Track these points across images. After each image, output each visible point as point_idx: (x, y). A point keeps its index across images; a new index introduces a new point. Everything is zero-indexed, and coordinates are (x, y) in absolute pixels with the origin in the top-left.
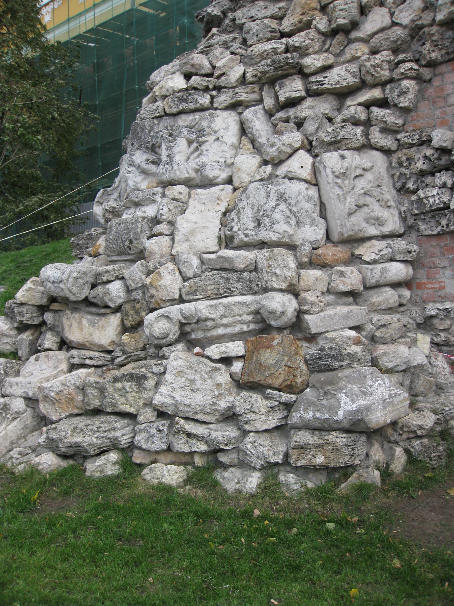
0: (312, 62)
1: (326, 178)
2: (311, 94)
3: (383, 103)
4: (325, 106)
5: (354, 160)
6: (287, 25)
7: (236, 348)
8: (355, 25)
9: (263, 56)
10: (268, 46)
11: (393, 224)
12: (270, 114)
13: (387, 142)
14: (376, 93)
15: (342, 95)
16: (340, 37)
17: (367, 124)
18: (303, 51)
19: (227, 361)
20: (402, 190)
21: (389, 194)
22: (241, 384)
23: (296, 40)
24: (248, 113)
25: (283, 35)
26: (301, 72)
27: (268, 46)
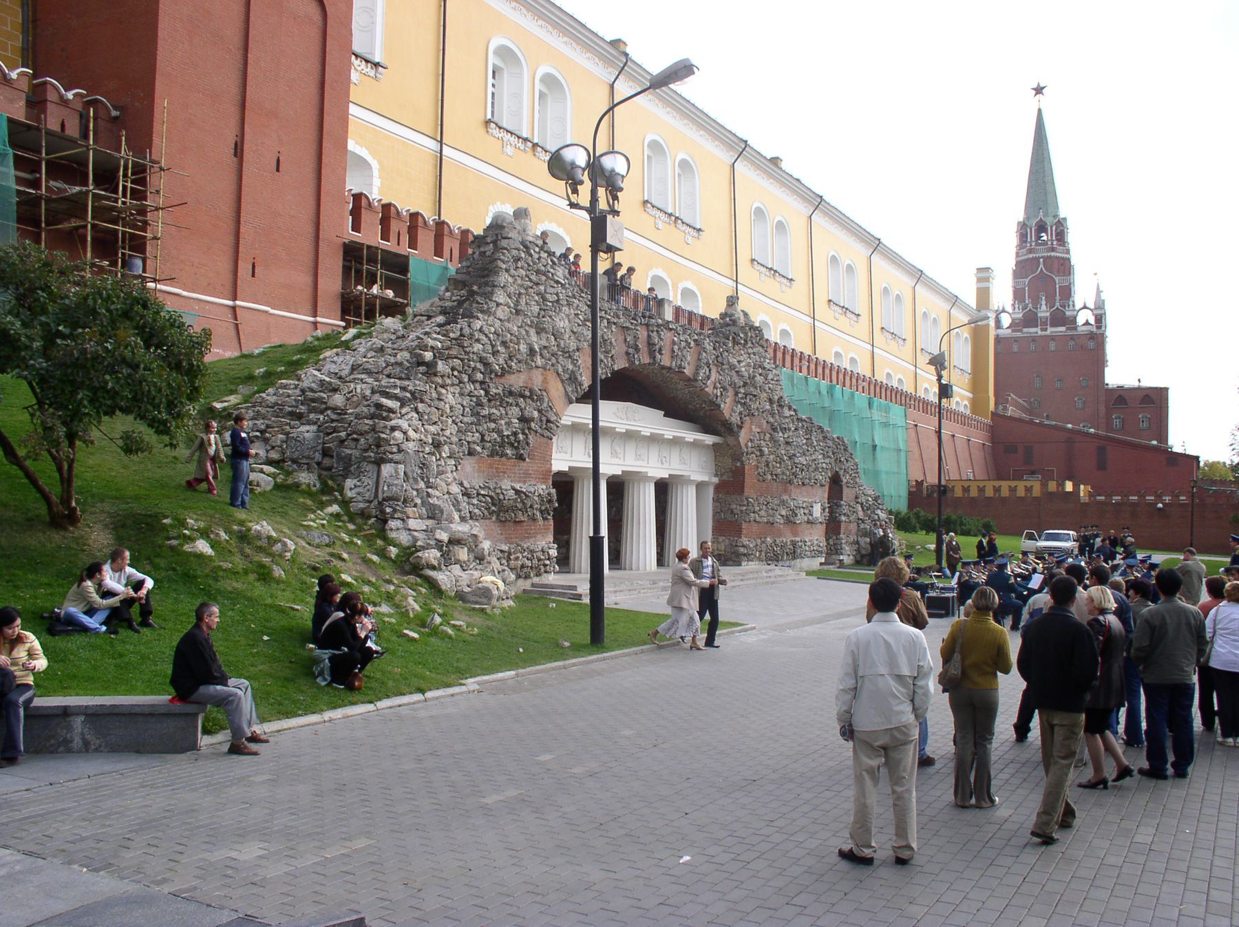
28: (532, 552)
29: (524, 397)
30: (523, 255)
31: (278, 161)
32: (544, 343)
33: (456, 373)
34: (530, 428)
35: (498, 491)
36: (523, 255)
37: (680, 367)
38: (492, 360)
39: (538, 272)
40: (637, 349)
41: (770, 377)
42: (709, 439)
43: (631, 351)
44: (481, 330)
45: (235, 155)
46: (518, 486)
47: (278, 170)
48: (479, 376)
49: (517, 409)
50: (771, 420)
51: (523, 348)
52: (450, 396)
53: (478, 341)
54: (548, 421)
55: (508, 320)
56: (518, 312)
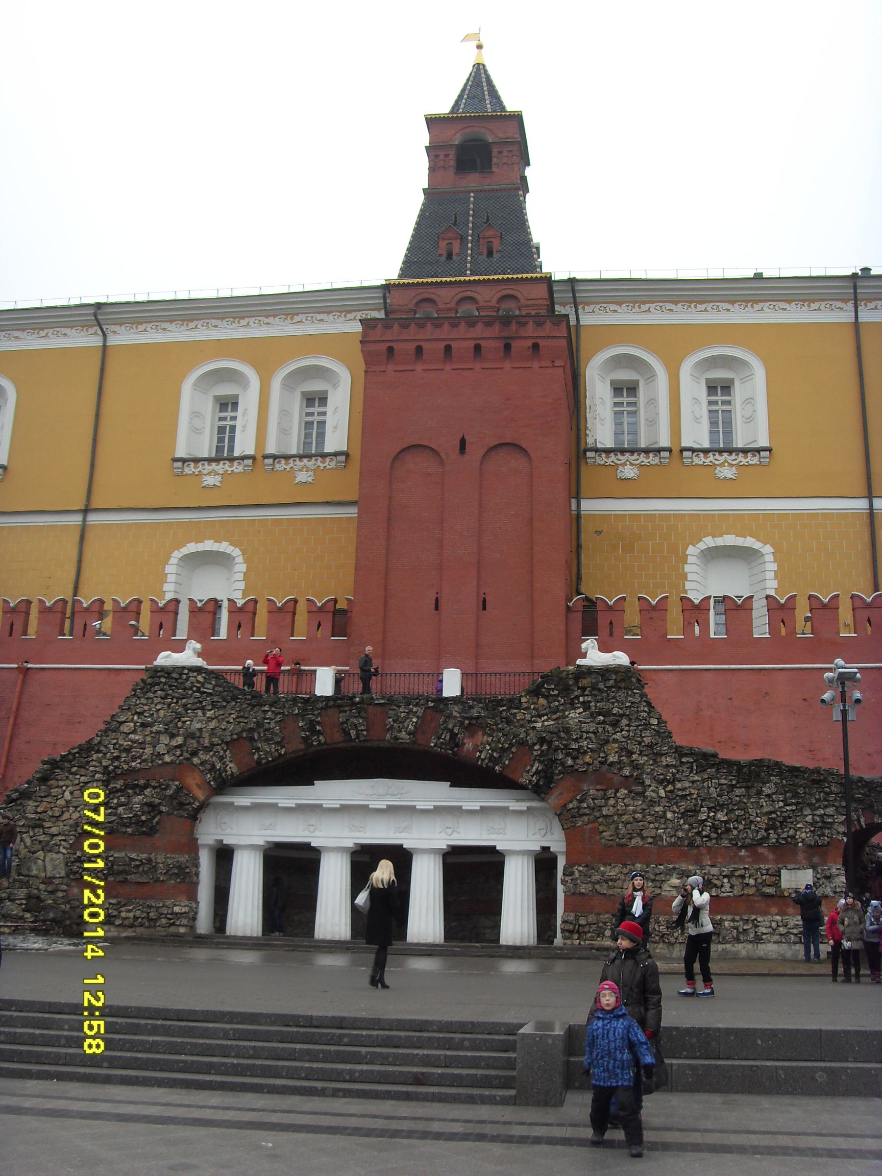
0: (47, 825)
1: (47, 859)
2: (44, 833)
3: (64, 840)
4: (47, 839)
5: (55, 856)
6: (39, 810)
7: (24, 902)
8: (60, 816)
9: (32, 819)
10: (33, 816)
11: (63, 874)
12: (31, 837)
13: (64, 851)
14: (63, 838)
15: (53, 836)
16: (54, 819)
17: (60, 845)
18: (44, 821)
19: (21, 904)
20: (66, 865)
21: (62, 865)
22: (24, 910)
23: (42, 816)
24: (24, 836)
25: (37, 813)
26: (42, 827)
27: (33, 816)
28: (150, 907)
29: (154, 788)
30: (163, 680)
31: (484, 601)
32: (174, 743)
33: (78, 777)
34: (161, 812)
35: (111, 859)
36: (163, 680)
37: (396, 738)
38: (105, 763)
39: (185, 689)
40: (319, 733)
41: (624, 722)
42: (523, 806)
43: (303, 734)
44: (100, 743)
45: (437, 608)
46: (133, 856)
47: (484, 609)
48: (97, 776)
49: (140, 797)
50: (626, 772)
51: (149, 750)
52: (67, 795)
53: (99, 751)
54: (181, 805)
55: (133, 732)
56: (144, 725)
